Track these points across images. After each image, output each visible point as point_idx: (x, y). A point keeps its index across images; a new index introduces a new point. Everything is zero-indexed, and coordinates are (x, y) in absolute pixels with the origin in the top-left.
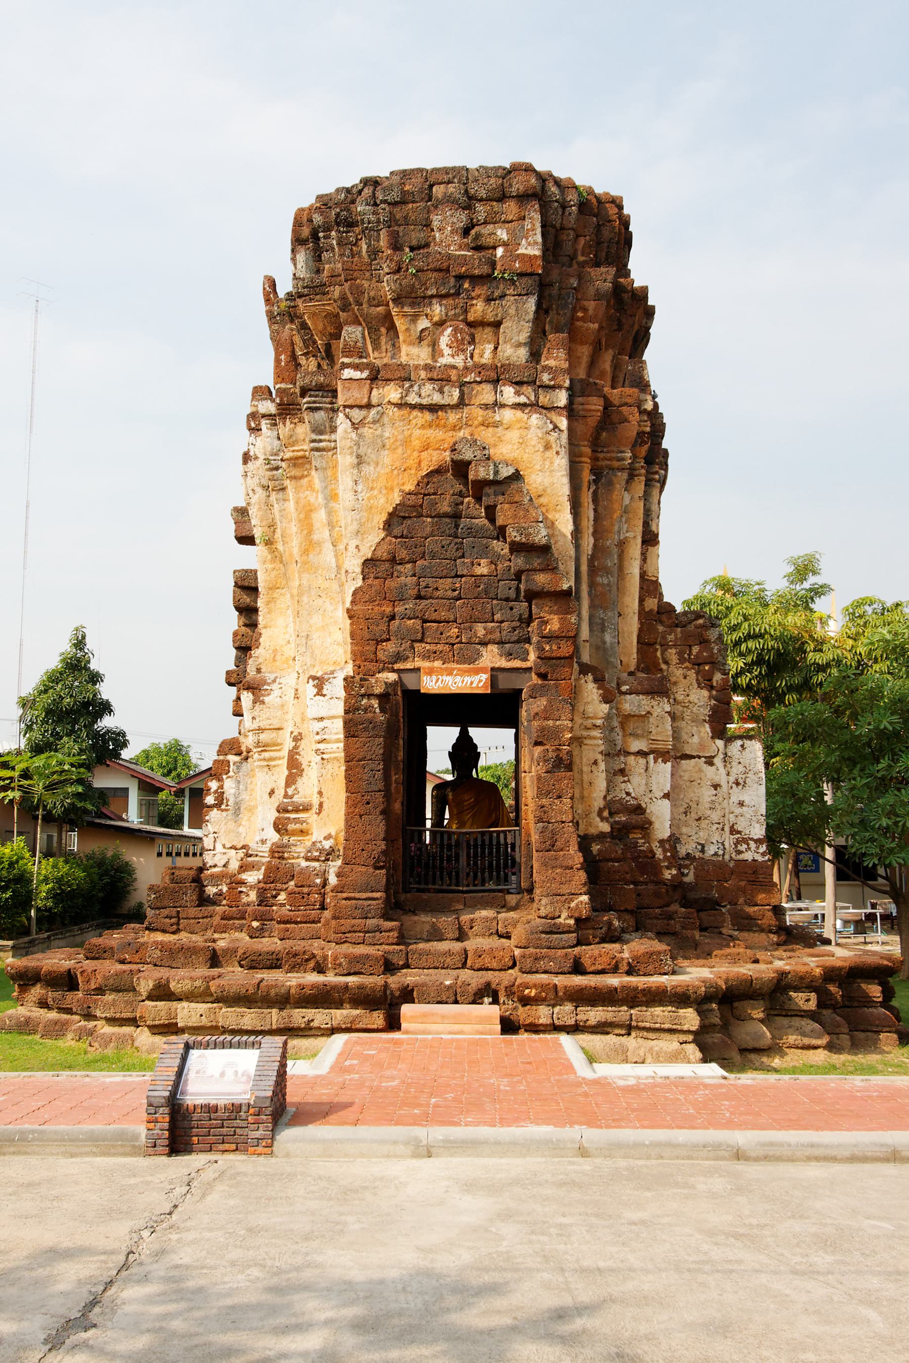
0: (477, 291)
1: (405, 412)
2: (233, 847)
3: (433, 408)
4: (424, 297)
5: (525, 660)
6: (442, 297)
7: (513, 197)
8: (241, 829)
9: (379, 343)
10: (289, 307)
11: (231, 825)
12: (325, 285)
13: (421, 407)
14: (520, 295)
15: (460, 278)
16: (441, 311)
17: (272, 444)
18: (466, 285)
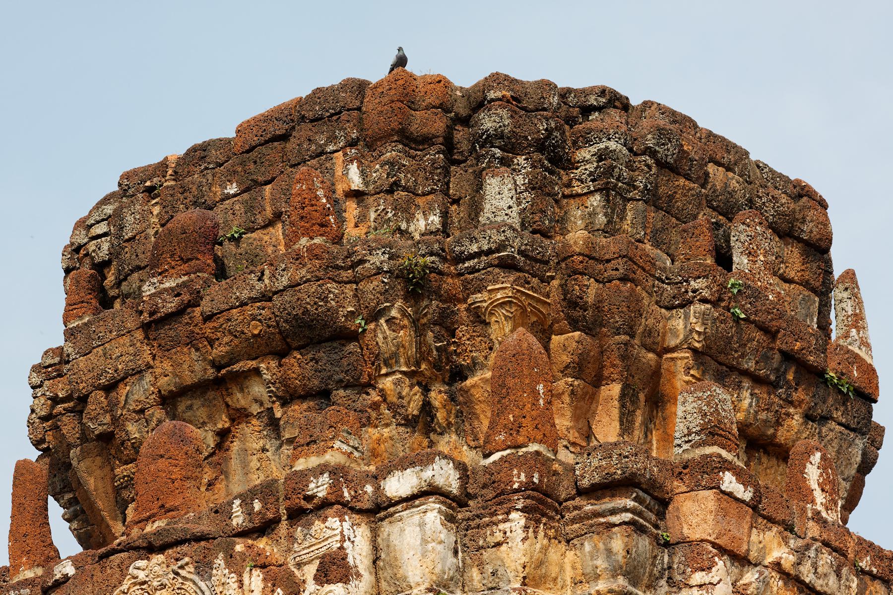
0: (799, 395)
4: (732, 368)
6: (757, 380)
7: (799, 240)
9: (632, 422)
10: (433, 270)
12: (547, 263)
14: (847, 427)
15: (788, 357)
16: (750, 405)
17: (444, 560)
18: (790, 376)
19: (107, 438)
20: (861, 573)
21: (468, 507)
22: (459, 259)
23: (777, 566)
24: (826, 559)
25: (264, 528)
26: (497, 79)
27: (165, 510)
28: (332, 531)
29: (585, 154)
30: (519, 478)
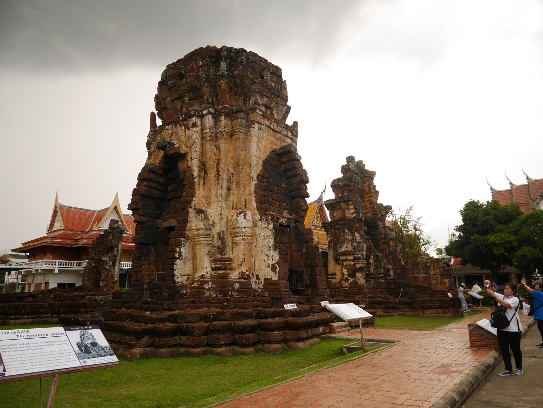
1: (269, 129)
2: (184, 275)
3: (275, 131)
5: (293, 216)
6: (267, 97)
8: (186, 268)
11: (183, 266)
13: (273, 129)
15: (272, 93)
19: (164, 108)
20: (281, 127)
21: (216, 117)
22: (217, 76)
23: (266, 125)
24: (275, 124)
25: (184, 120)
26: (224, 46)
27: (171, 118)
28: (194, 119)
29: (239, 59)
30: (223, 110)
